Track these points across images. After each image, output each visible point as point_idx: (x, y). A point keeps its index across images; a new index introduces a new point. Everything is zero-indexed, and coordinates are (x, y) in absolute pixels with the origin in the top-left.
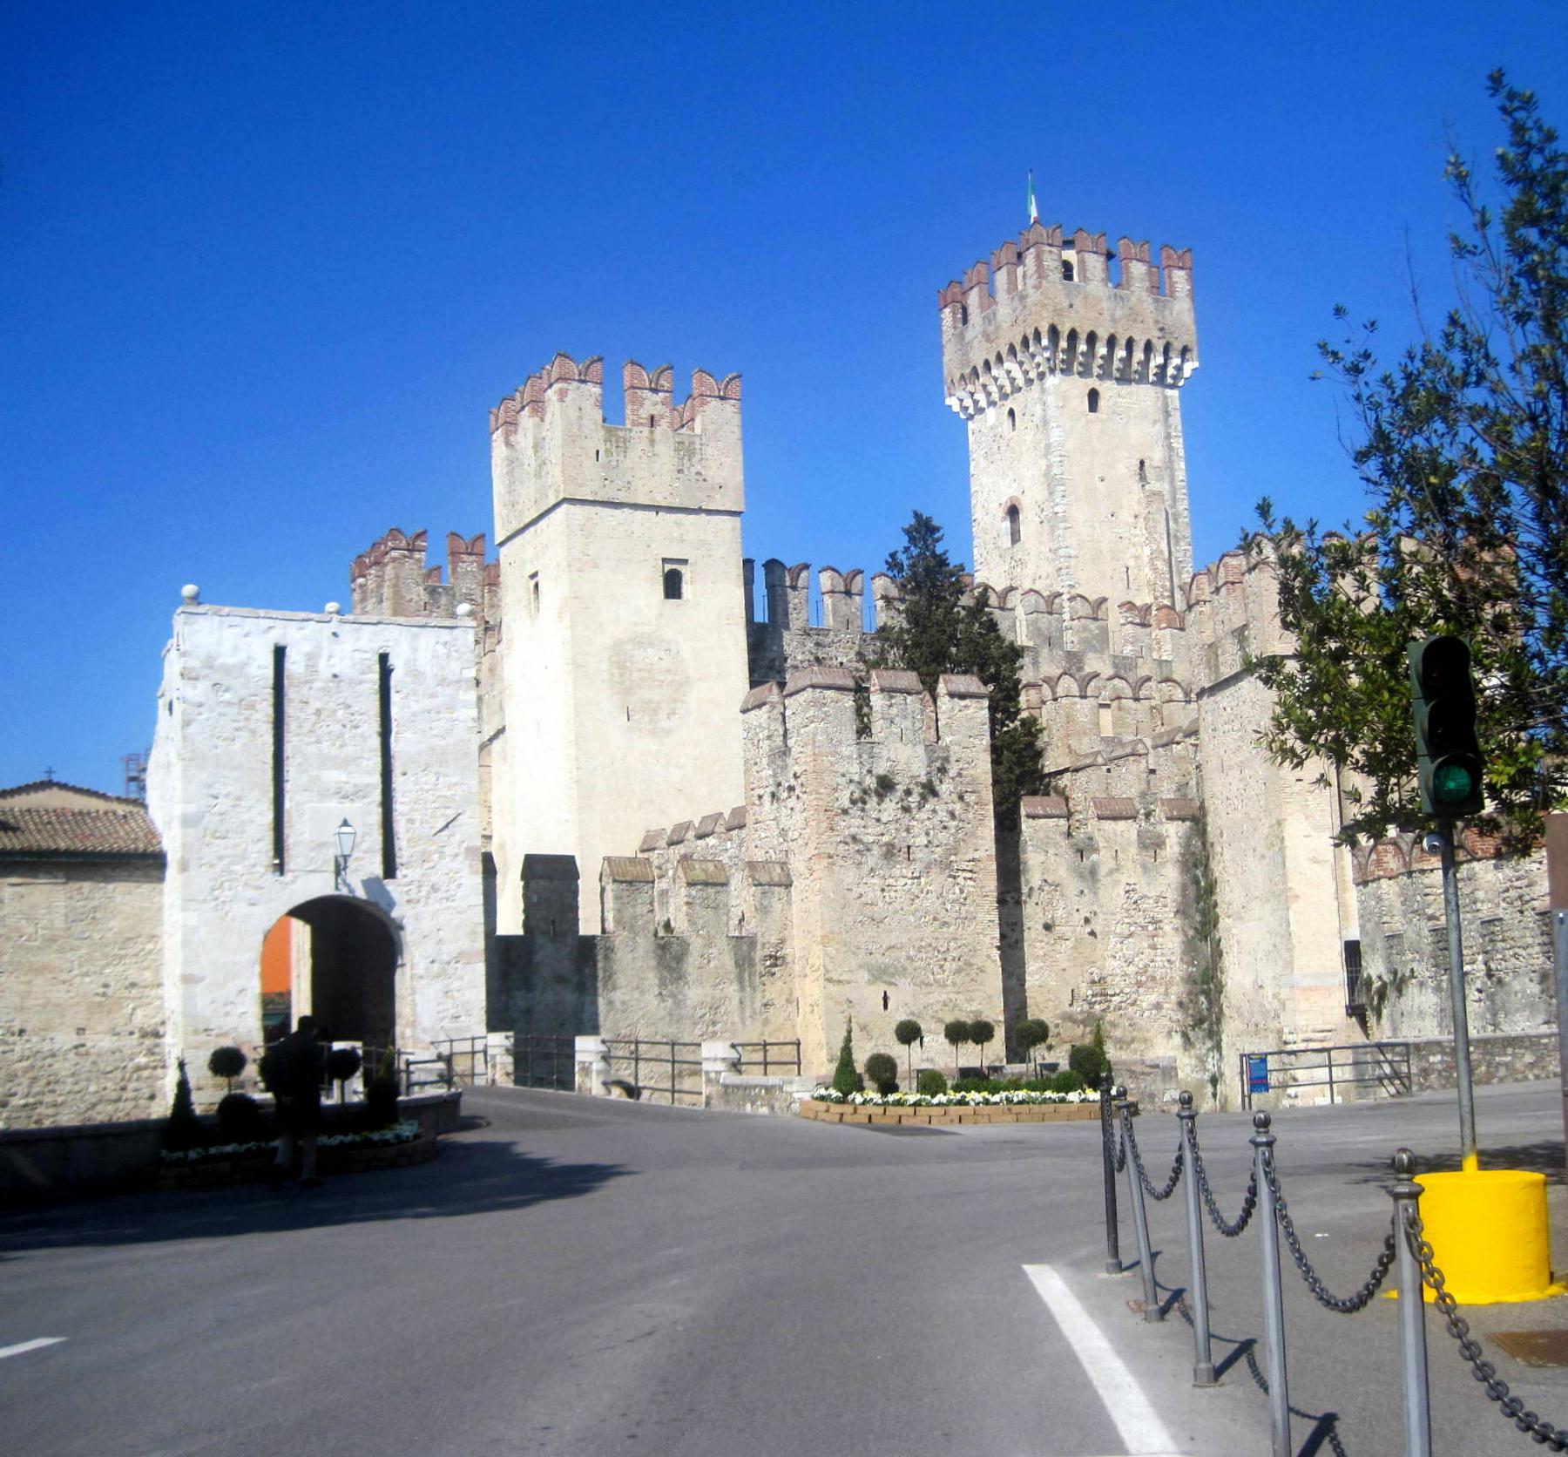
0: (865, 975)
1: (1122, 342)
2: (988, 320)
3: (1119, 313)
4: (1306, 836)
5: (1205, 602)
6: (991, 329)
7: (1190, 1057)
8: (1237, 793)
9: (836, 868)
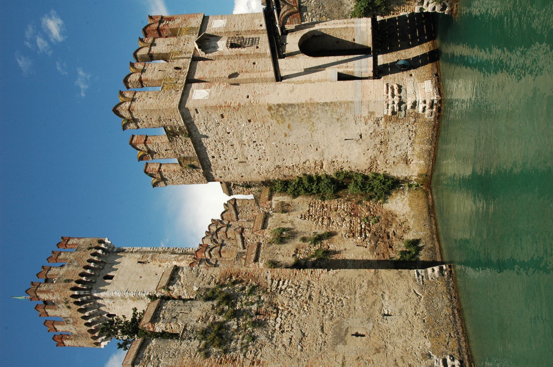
0: (340, 347)
1: (88, 264)
2: (67, 322)
3: (76, 264)
4: (278, 95)
5: (160, 168)
6: (72, 321)
7: (396, 196)
8: (256, 149)
9: (262, 360)
